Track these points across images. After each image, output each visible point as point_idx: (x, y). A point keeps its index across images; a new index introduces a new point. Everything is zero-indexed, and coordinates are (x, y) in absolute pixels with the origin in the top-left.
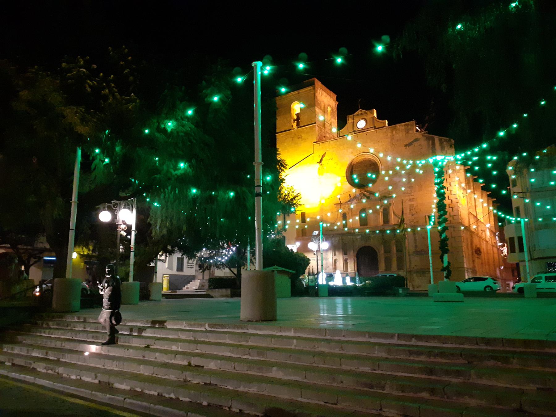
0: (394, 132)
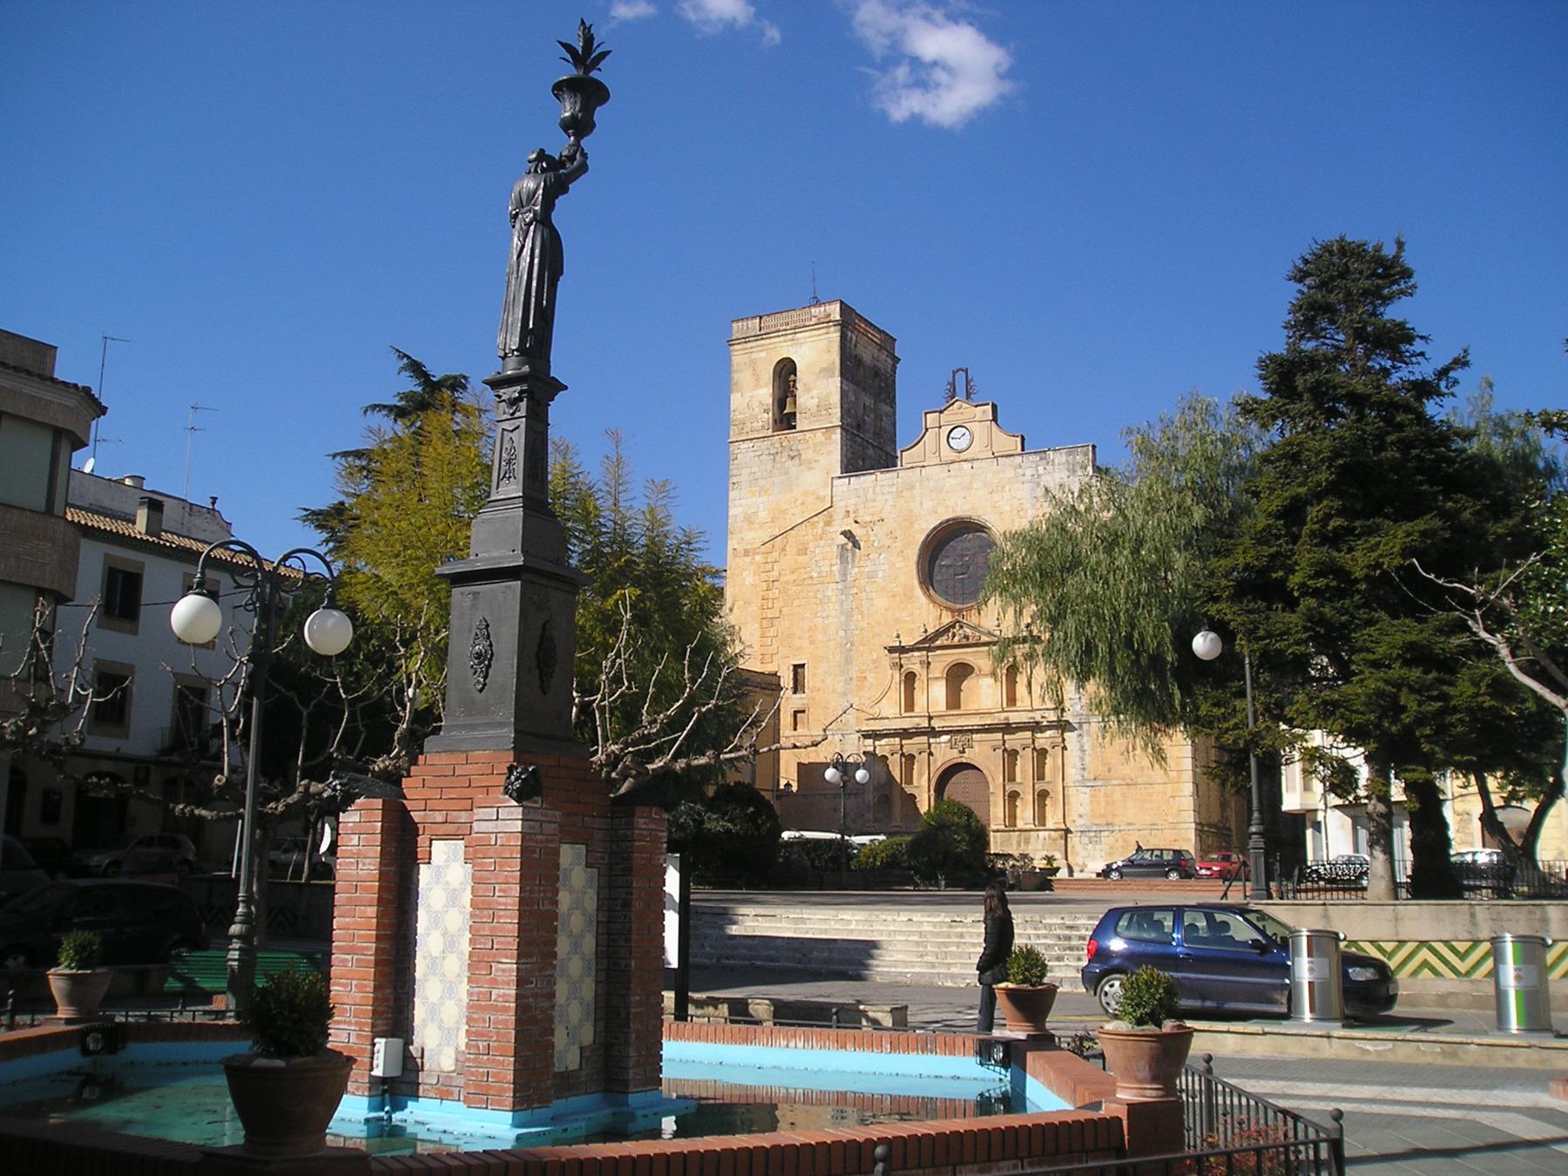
0: (1041, 469)
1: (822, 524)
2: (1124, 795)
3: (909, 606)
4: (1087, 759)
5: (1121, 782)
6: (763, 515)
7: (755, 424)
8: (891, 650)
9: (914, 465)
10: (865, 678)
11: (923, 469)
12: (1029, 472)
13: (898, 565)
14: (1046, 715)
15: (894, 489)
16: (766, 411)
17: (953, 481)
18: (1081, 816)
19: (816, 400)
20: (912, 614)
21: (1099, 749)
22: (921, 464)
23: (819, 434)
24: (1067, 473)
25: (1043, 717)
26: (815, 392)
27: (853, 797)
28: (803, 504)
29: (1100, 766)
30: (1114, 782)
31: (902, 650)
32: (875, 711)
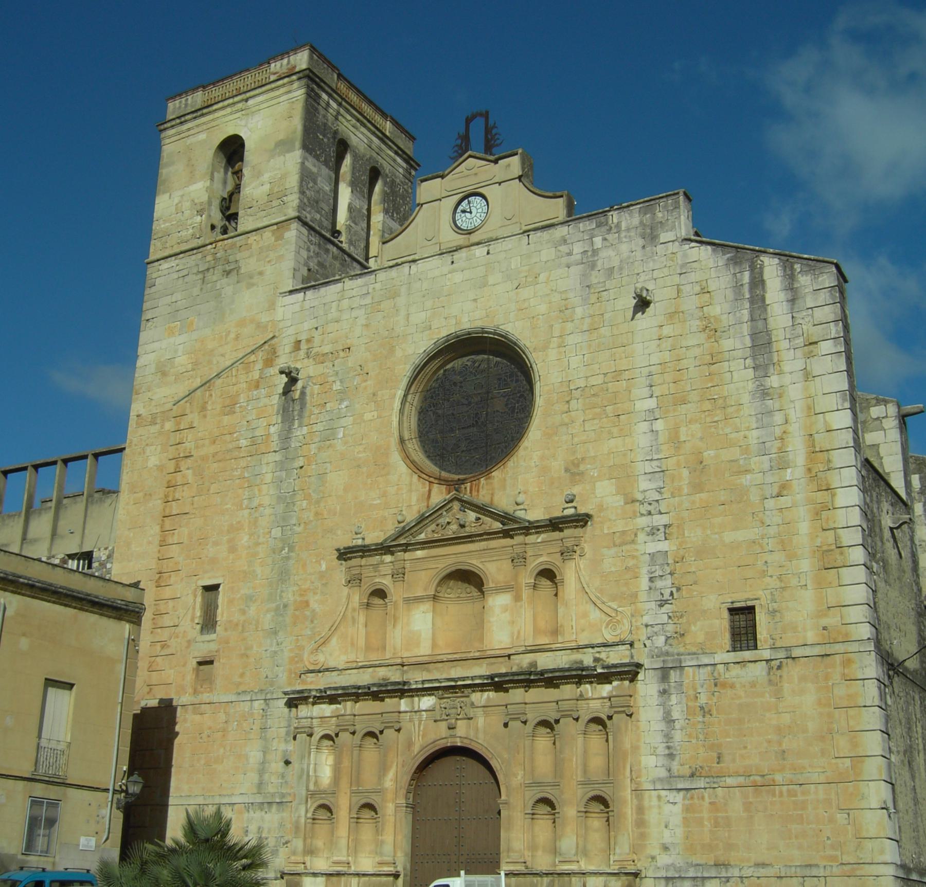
0: (598, 241)
1: (259, 365)
2: (747, 806)
3: (380, 479)
4: (678, 736)
5: (741, 780)
6: (182, 361)
7: (183, 233)
8: (345, 554)
9: (399, 261)
10: (307, 604)
11: (414, 266)
12: (578, 249)
13: (368, 416)
14: (603, 656)
15: (368, 300)
16: (200, 213)
17: (458, 277)
18: (666, 848)
19: (267, 187)
20: (384, 495)
21: (700, 719)
22: (410, 258)
23: (267, 234)
24: (641, 242)
25: (596, 660)
26: (266, 177)
27: (274, 807)
28: (237, 338)
29: (701, 750)
30: (730, 781)
31: (364, 551)
32: (322, 659)
